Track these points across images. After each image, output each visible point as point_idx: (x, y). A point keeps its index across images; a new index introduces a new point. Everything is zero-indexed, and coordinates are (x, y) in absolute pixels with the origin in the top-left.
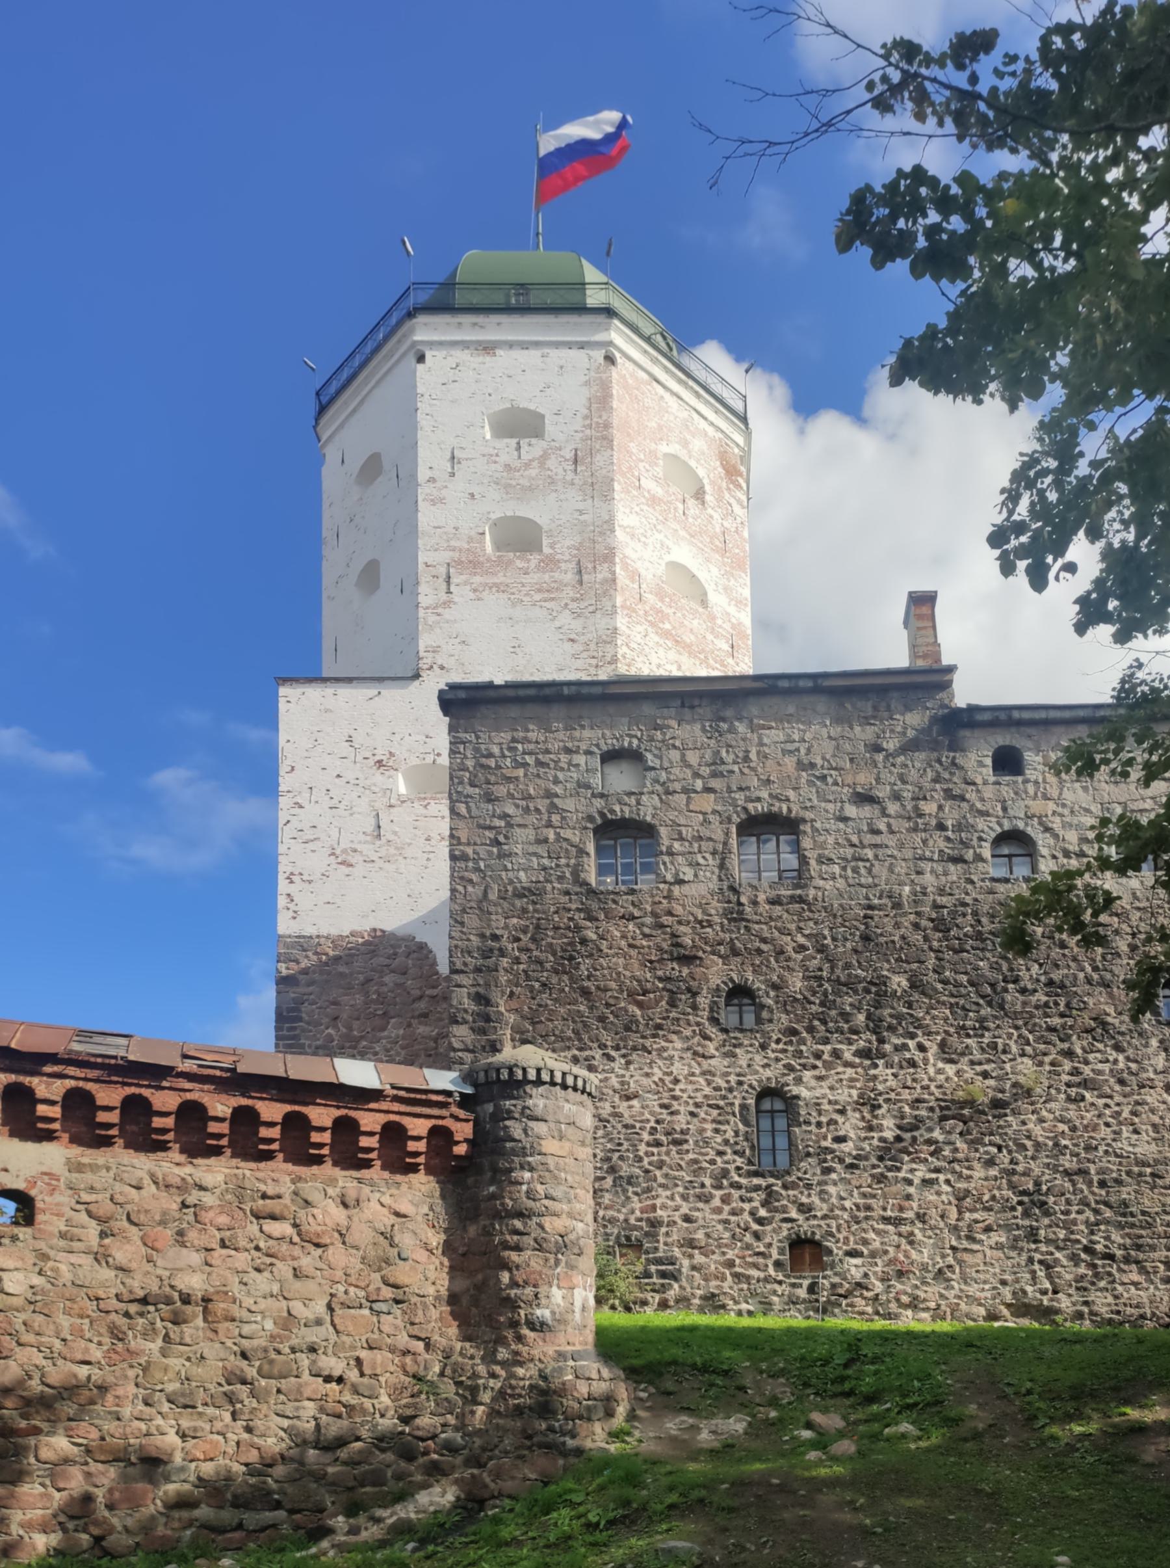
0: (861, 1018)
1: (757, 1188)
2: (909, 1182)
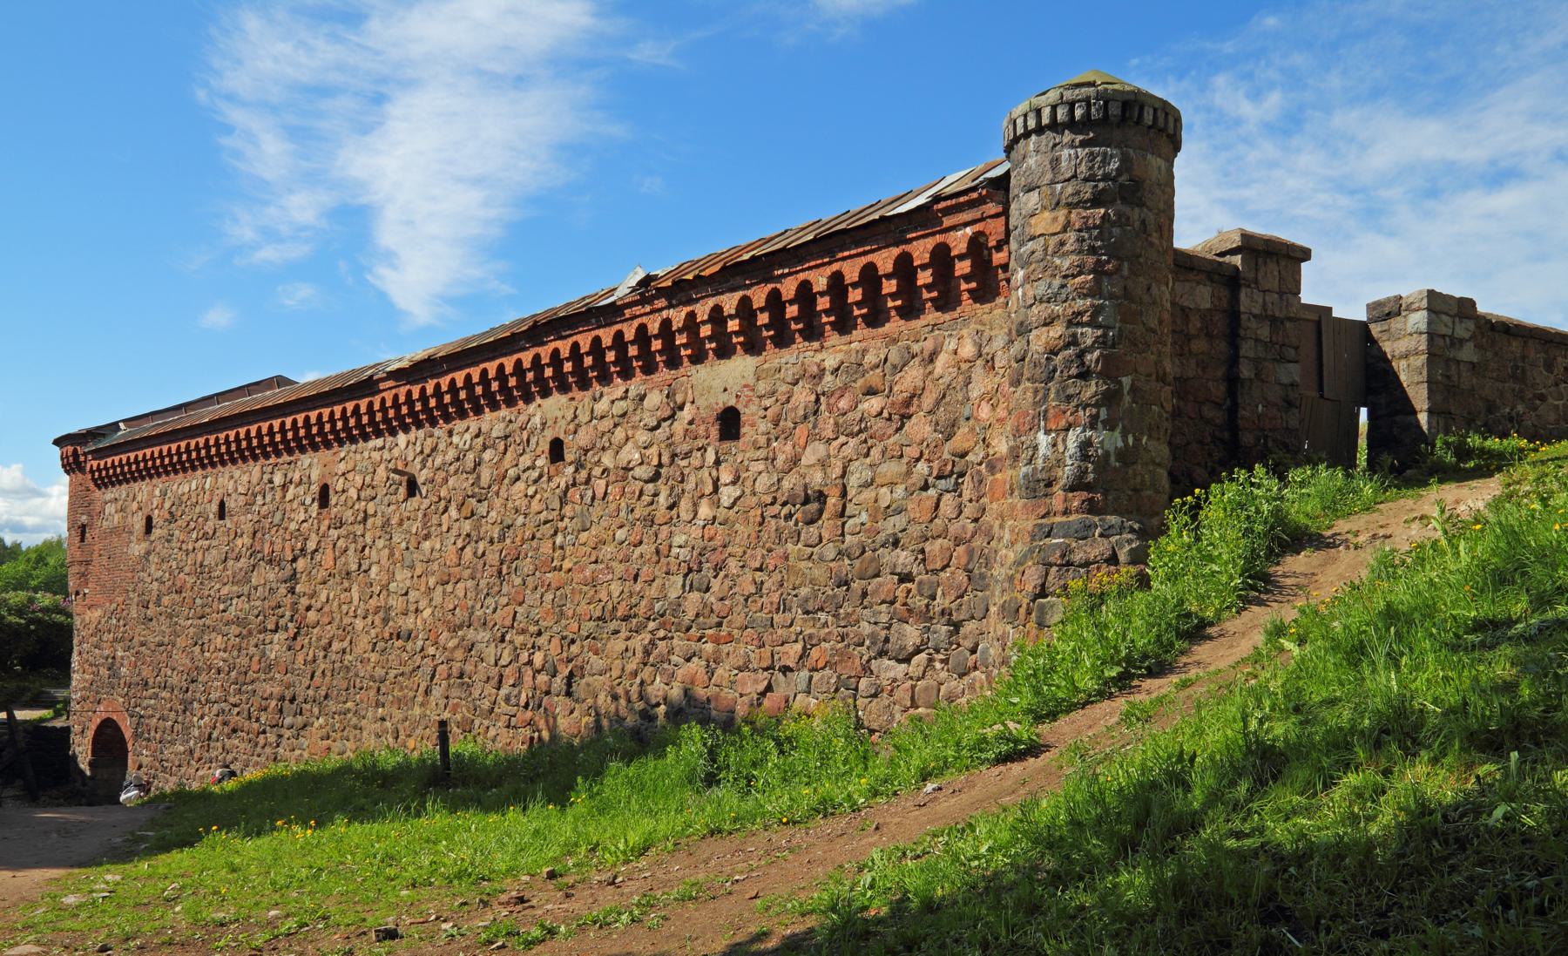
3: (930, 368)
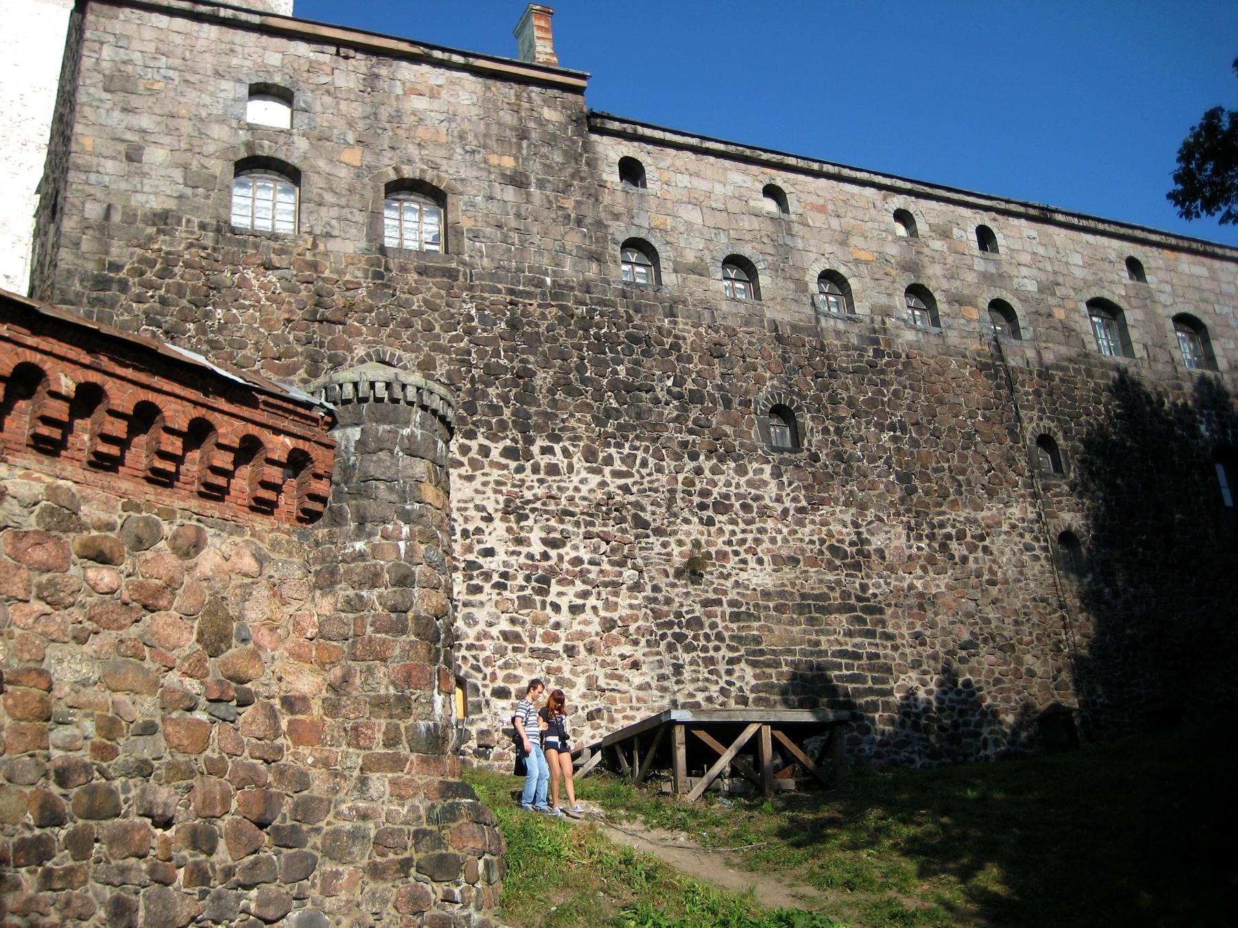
0: (507, 413)
2: (556, 608)
3: (189, 563)
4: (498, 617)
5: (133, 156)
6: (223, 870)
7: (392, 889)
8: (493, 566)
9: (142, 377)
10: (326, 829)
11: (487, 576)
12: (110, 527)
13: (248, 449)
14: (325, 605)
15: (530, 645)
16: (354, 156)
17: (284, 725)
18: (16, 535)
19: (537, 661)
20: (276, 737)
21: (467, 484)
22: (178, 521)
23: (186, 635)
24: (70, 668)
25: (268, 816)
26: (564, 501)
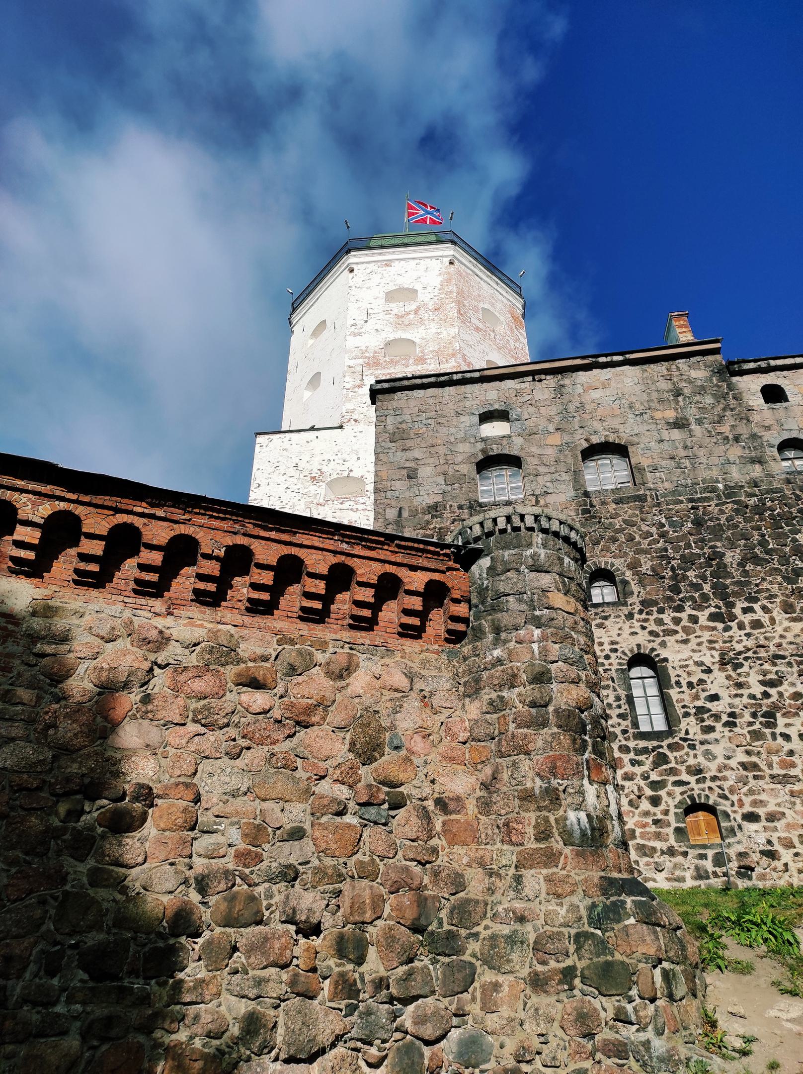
0: (707, 588)
1: (645, 751)
2: (787, 737)
4: (734, 751)
5: (412, 475)
6: (373, 981)
7: (556, 1005)
8: (720, 709)
9: (285, 537)
10: (484, 934)
11: (717, 717)
12: (265, 659)
13: (388, 587)
14: (474, 709)
15: (768, 772)
16: (556, 439)
17: (438, 826)
18: (176, 670)
19: (779, 786)
20: (431, 837)
21: (683, 646)
22: (331, 650)
23: (338, 746)
24: (218, 780)
25: (423, 922)
26: (772, 649)
